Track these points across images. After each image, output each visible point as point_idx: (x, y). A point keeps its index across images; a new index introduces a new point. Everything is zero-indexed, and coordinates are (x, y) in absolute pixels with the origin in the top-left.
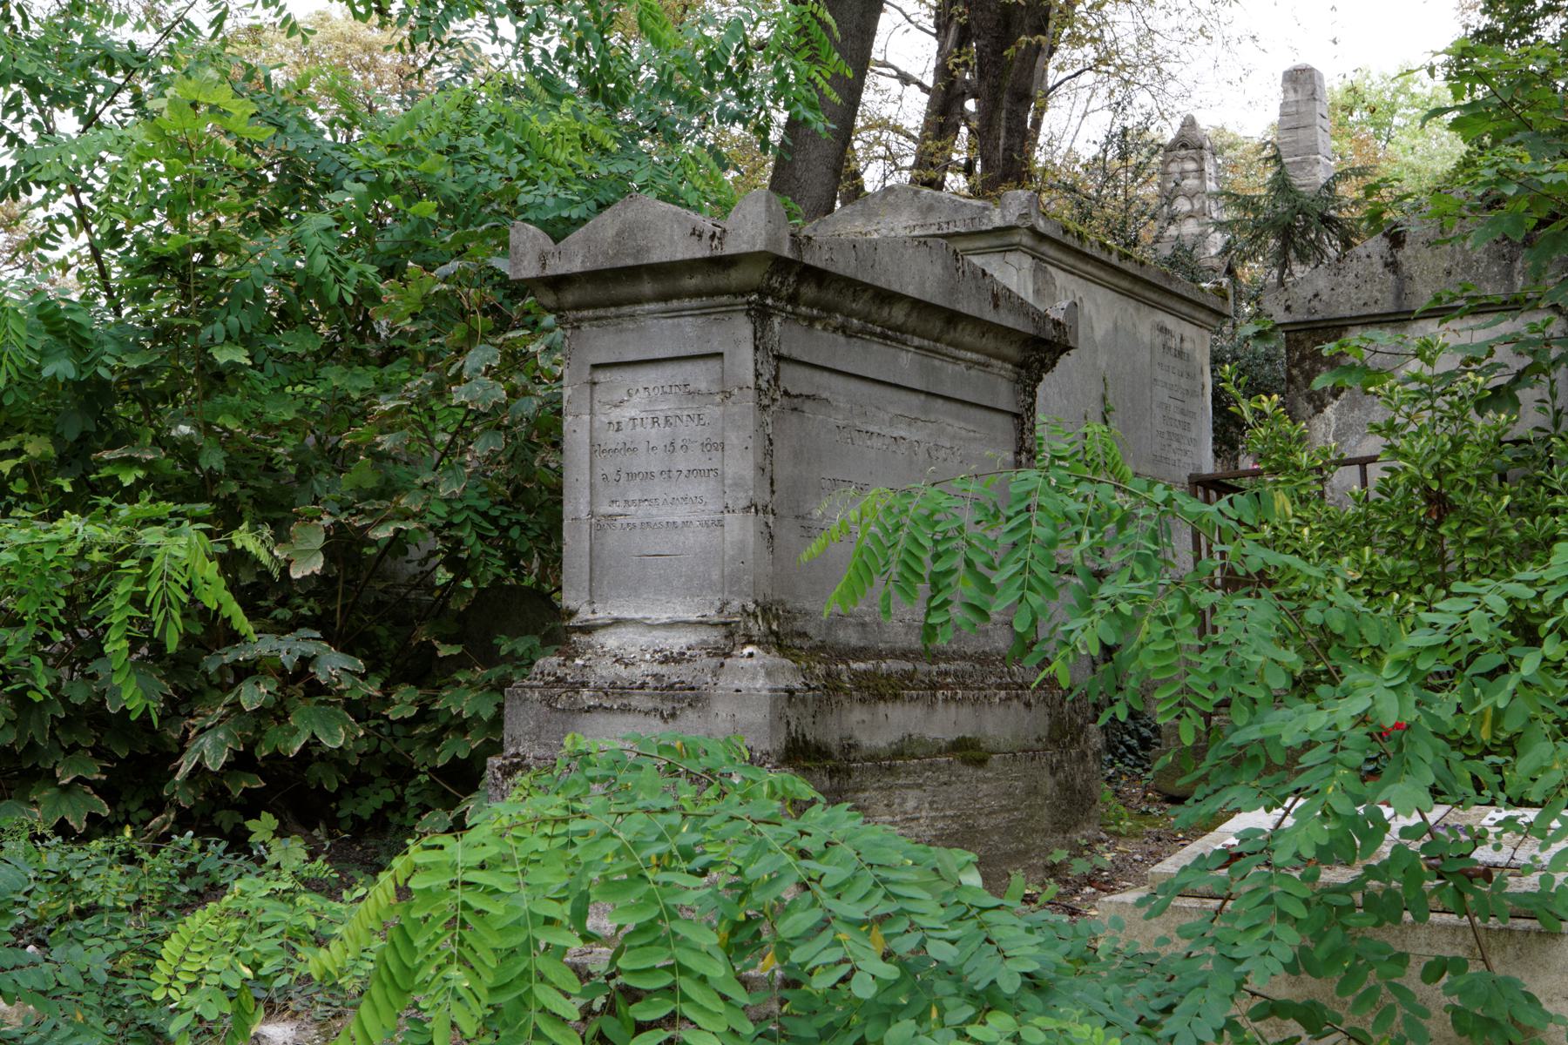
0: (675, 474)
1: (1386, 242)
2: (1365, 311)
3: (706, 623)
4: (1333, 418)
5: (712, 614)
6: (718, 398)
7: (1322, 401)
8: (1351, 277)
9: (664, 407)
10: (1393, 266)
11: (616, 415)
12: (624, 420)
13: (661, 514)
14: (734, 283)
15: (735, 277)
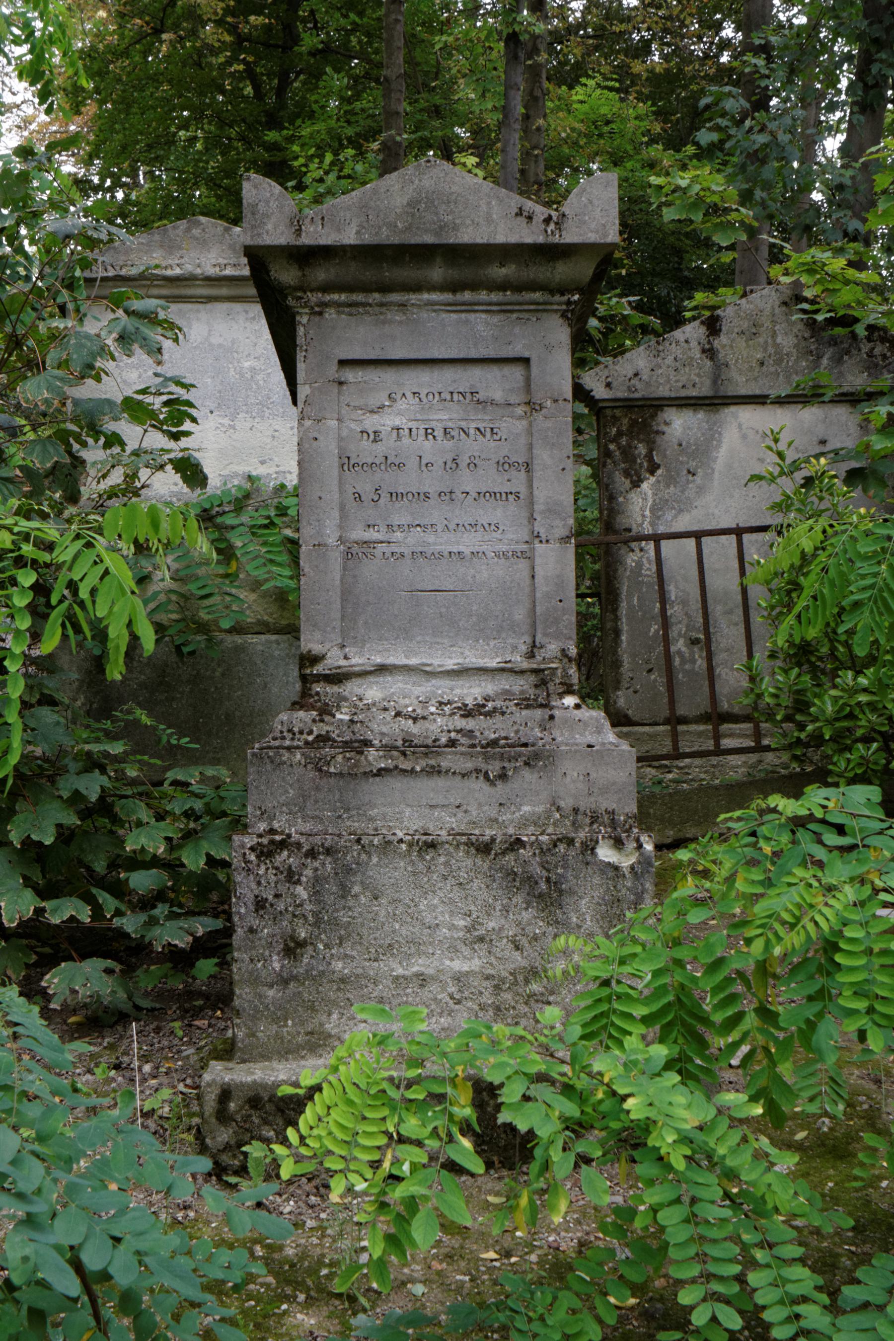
0: (458, 495)
1: (703, 330)
2: (684, 393)
3: (512, 671)
4: (650, 493)
5: (518, 660)
6: (519, 411)
7: (639, 476)
8: (670, 360)
9: (441, 417)
10: (710, 352)
11: (371, 422)
12: (385, 430)
13: (440, 542)
14: (557, 278)
15: (562, 271)
